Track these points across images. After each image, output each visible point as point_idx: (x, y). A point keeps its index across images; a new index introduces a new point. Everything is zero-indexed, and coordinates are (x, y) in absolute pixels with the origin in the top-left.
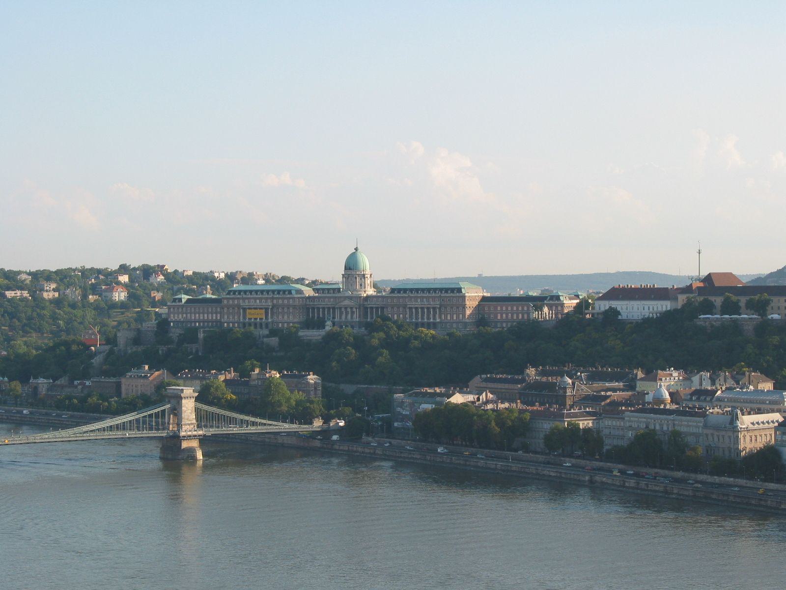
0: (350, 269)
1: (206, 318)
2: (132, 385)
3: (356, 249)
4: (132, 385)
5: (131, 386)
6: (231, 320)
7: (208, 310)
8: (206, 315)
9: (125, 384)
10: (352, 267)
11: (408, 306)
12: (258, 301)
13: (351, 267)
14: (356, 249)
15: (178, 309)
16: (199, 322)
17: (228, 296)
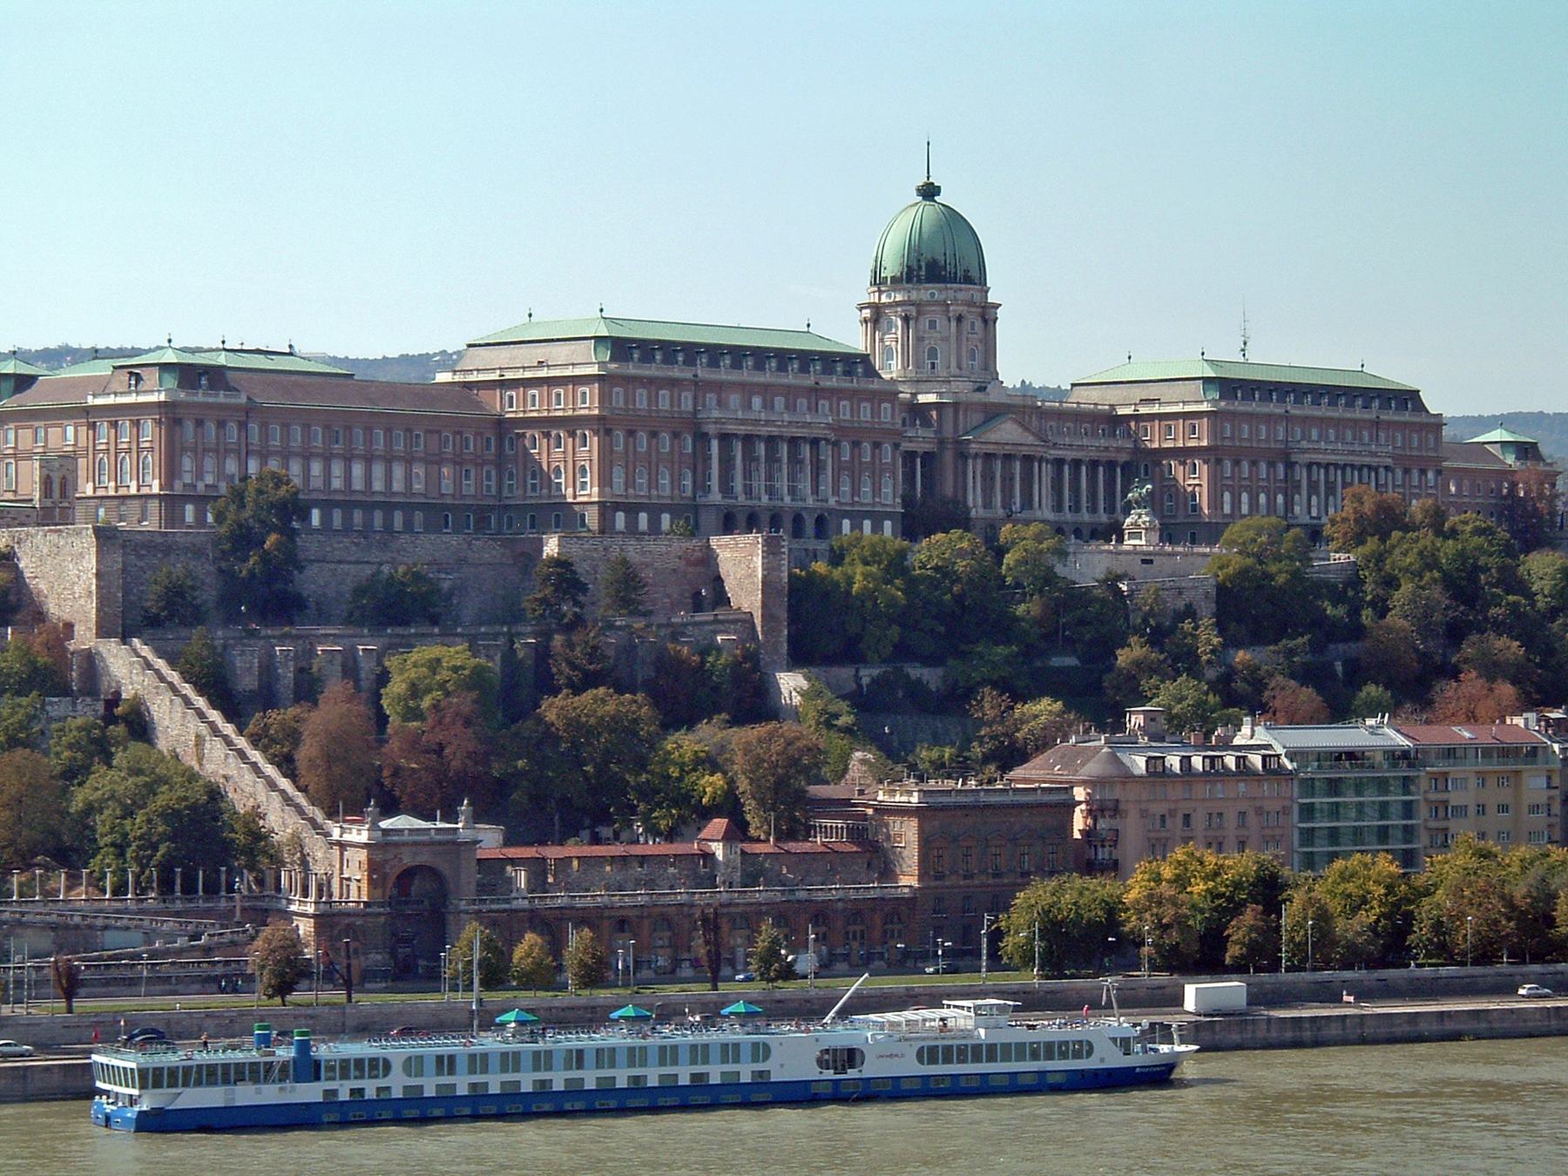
0: (968, 280)
1: (358, 485)
2: (1187, 817)
3: (929, 192)
4: (1187, 817)
5: (1179, 820)
6: (641, 492)
7: (369, 440)
8: (358, 470)
9: (1144, 814)
10: (974, 274)
11: (1308, 457)
12: (757, 402)
13: (941, 272)
14: (929, 192)
15: (221, 424)
16: (327, 506)
17: (631, 369)
